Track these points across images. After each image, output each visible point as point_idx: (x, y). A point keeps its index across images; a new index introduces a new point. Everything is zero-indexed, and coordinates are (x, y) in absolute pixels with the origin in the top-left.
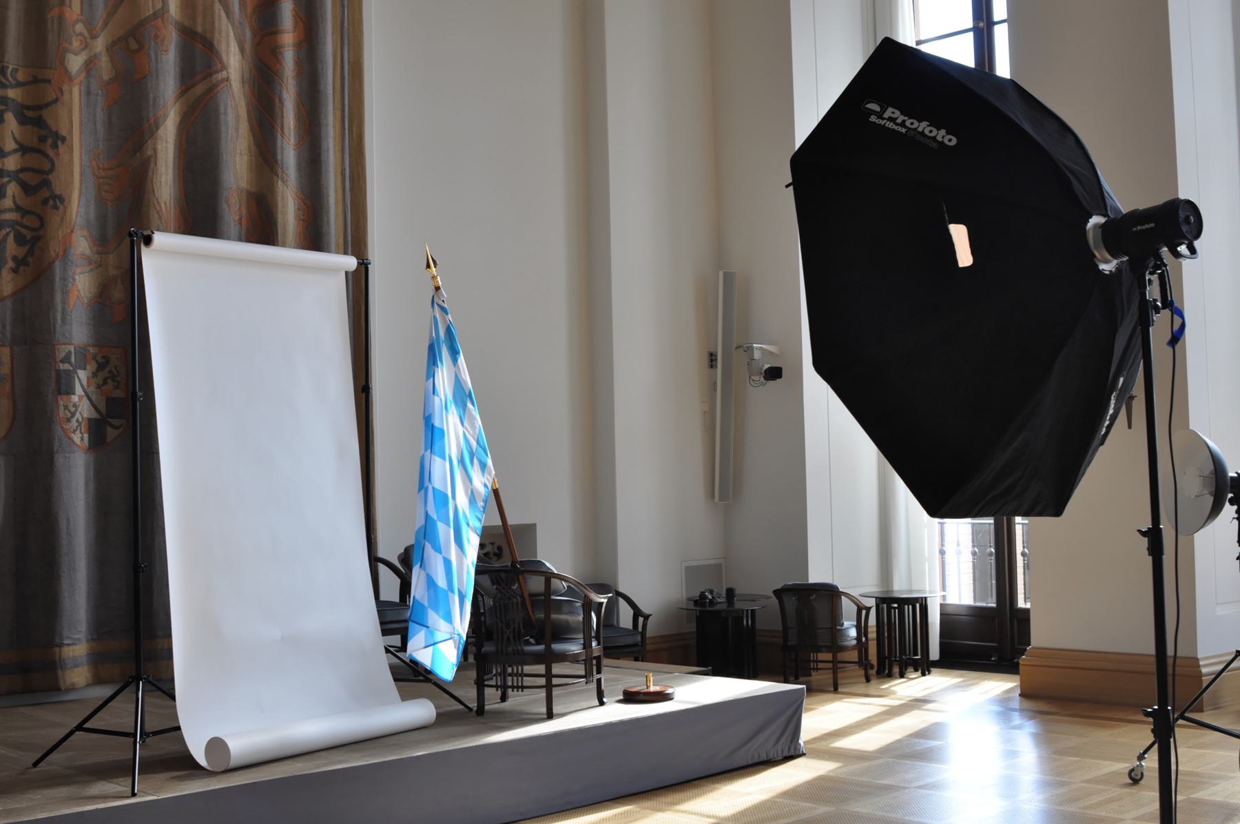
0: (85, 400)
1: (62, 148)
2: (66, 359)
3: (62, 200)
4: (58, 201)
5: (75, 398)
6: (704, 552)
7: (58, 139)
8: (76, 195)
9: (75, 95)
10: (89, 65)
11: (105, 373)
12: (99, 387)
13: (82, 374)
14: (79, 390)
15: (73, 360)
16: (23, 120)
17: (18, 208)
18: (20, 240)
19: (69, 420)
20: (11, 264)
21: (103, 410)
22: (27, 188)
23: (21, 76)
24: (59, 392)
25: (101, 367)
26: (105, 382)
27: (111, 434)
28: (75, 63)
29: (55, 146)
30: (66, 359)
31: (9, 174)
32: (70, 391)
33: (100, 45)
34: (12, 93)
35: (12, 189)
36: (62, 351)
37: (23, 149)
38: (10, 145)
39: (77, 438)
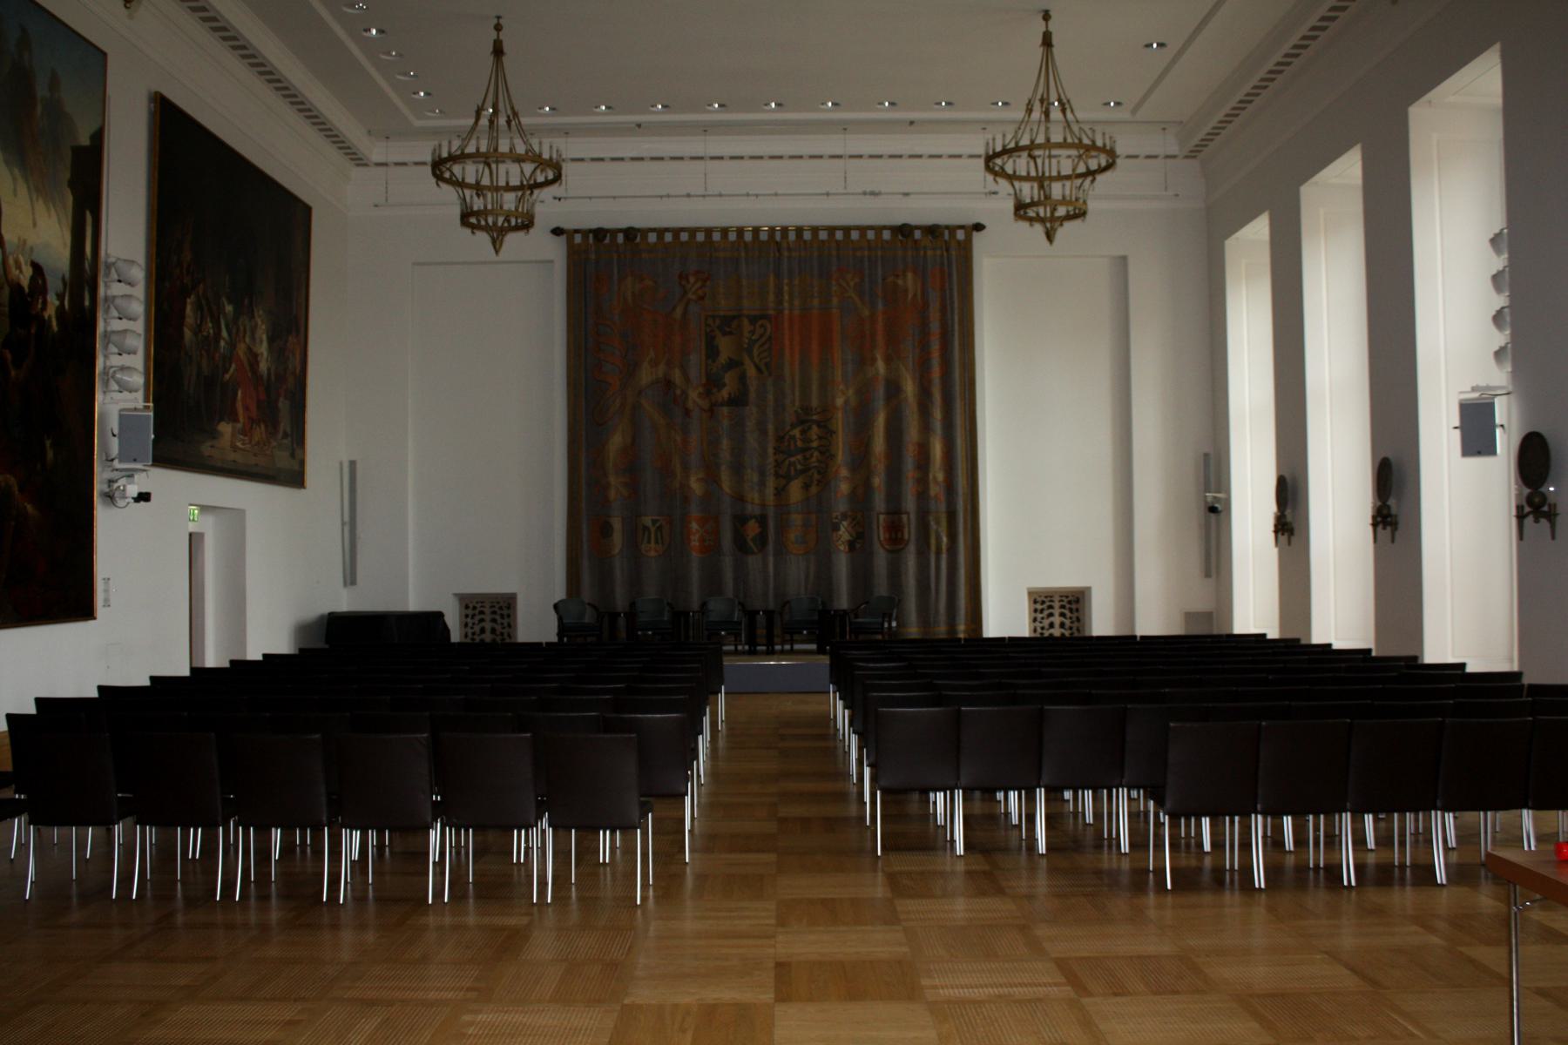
0: (847, 534)
1: (834, 436)
2: (836, 518)
3: (834, 456)
4: (833, 457)
5: (841, 533)
6: (1200, 605)
7: (832, 432)
8: (840, 453)
9: (840, 415)
10: (846, 402)
11: (854, 522)
12: (852, 527)
13: (845, 523)
14: (842, 529)
15: (839, 517)
16: (819, 426)
17: (818, 461)
18: (819, 473)
19: (838, 541)
20: (816, 482)
21: (854, 535)
22: (821, 452)
23: (819, 410)
24: (833, 530)
25: (853, 519)
26: (855, 525)
27: (858, 546)
28: (839, 402)
29: (831, 435)
30: (836, 518)
31: (813, 448)
32: (839, 529)
33: (851, 392)
34: (815, 417)
35: (816, 454)
36: (834, 515)
37: (820, 438)
38: (815, 437)
39: (842, 548)
